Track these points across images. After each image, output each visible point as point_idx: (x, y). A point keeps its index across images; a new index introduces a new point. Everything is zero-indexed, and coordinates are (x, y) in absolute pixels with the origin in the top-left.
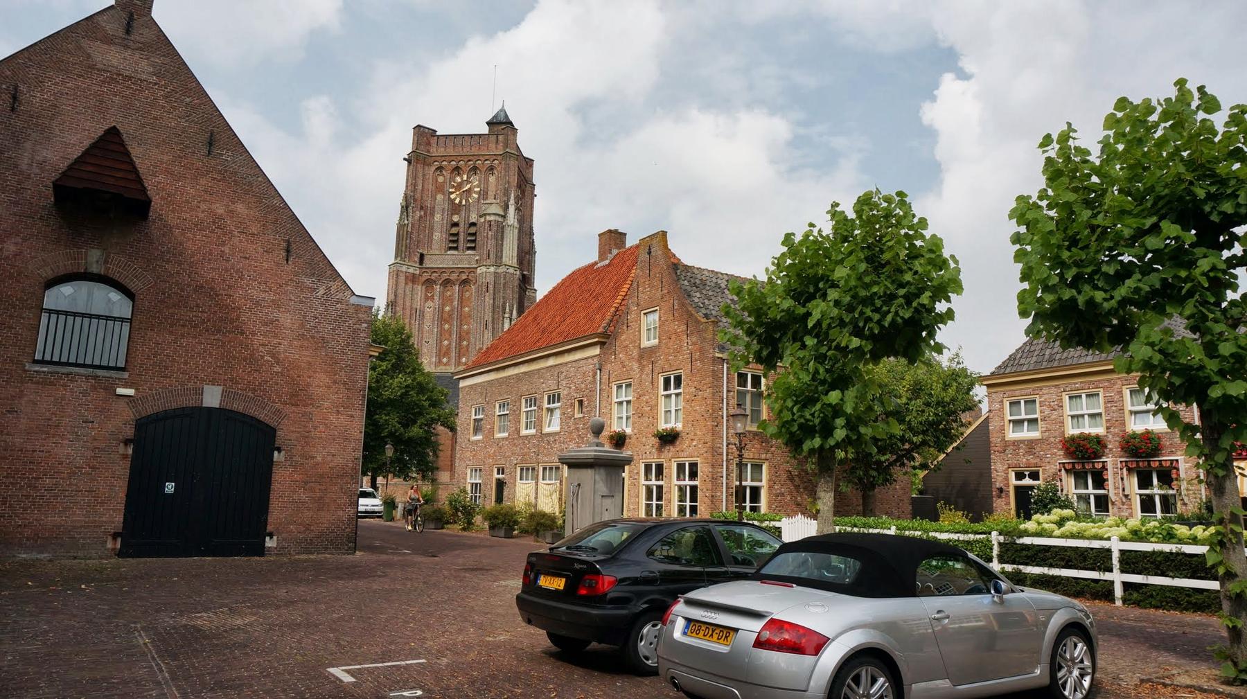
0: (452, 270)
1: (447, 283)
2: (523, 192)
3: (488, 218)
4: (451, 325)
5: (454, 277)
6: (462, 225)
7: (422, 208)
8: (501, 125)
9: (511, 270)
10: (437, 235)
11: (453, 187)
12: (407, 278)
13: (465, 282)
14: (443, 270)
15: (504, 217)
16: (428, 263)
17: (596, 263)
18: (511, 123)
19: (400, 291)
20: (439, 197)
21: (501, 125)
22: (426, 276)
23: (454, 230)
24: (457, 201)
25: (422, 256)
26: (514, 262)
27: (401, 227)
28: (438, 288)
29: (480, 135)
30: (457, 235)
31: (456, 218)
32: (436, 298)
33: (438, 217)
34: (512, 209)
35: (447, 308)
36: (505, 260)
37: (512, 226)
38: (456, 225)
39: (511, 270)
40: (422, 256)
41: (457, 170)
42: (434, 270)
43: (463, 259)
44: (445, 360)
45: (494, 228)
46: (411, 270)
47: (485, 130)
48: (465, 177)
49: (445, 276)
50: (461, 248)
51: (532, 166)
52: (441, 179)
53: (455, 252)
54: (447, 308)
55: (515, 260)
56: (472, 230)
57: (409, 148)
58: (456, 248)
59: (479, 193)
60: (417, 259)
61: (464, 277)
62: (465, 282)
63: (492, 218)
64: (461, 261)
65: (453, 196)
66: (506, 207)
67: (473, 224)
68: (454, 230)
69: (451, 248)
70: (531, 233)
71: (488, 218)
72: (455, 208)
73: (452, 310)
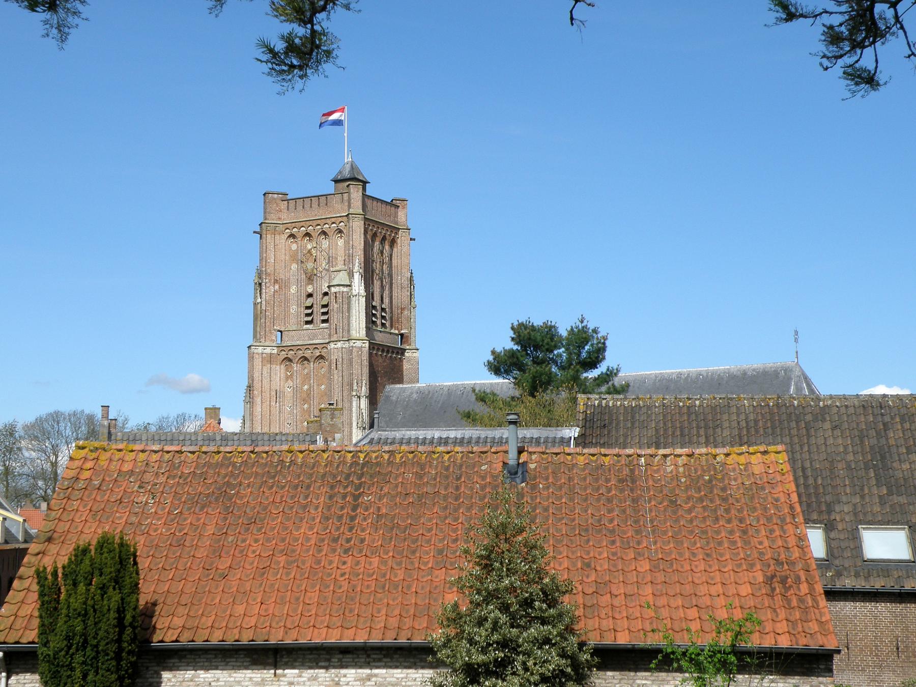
0: (307, 347)
5: (308, 354)
7: (276, 281)
9: (359, 344)
10: (293, 309)
14: (298, 347)
19: (257, 375)
23: (309, 302)
26: (363, 333)
31: (310, 289)
33: (293, 289)
35: (306, 387)
36: (354, 334)
37: (359, 295)
38: (310, 295)
42: (291, 348)
43: (317, 334)
46: (268, 350)
54: (306, 387)
56: (325, 300)
64: (315, 336)
67: (326, 294)
69: (307, 323)
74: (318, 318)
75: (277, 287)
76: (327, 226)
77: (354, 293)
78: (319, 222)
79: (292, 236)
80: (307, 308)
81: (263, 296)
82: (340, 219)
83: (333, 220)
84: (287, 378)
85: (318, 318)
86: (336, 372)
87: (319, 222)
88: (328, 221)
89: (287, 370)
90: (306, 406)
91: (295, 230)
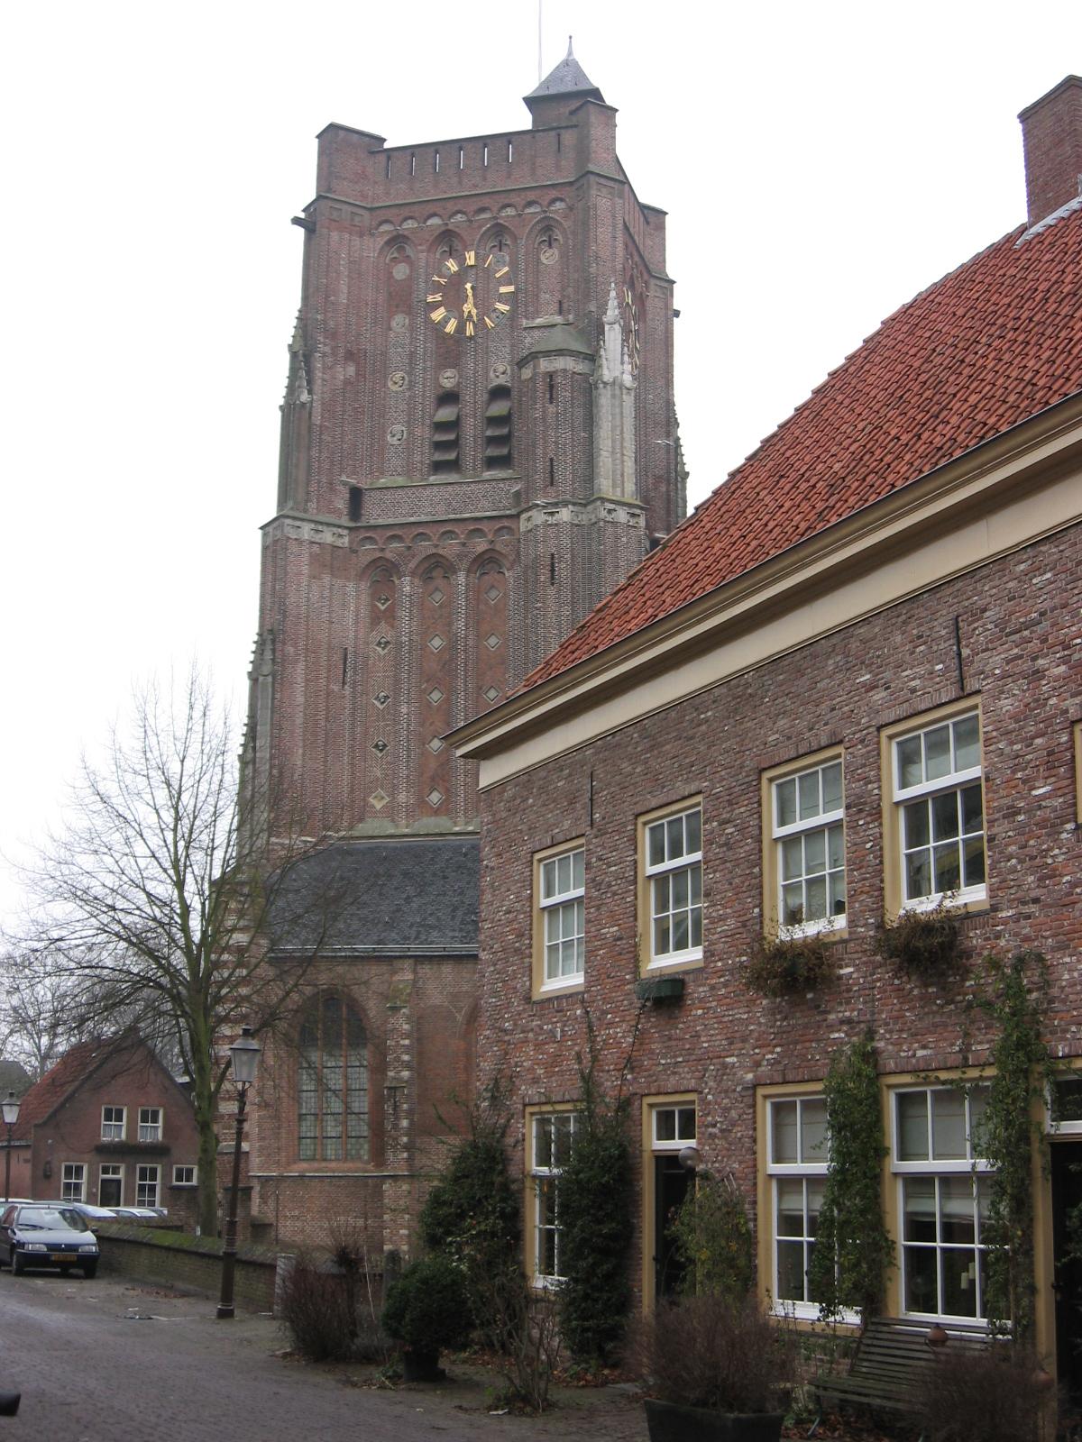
1: (435, 567)
2: (641, 300)
3: (544, 365)
4: (451, 691)
5: (450, 548)
6: (467, 397)
7: (350, 356)
8: (571, 110)
10: (396, 433)
11: (437, 288)
12: (314, 558)
13: (487, 562)
14: (419, 530)
15: (593, 358)
16: (374, 514)
17: (1023, 229)
18: (596, 93)
20: (399, 321)
21: (571, 110)
22: (369, 552)
23: (446, 414)
24: (451, 327)
25: (356, 495)
27: (293, 413)
28: (407, 585)
29: (508, 138)
30: (453, 425)
31: (448, 380)
32: (403, 614)
33: (396, 382)
34: (613, 337)
35: (437, 642)
36: (605, 485)
38: (449, 398)
39: (622, 515)
40: (356, 495)
41: (449, 241)
42: (394, 532)
43: (481, 493)
44: (435, 797)
45: (564, 394)
46: (327, 537)
47: (523, 120)
48: (471, 258)
49: (425, 548)
50: (468, 461)
51: (661, 227)
52: (401, 272)
53: (453, 477)
54: (437, 642)
55: (630, 487)
56: (499, 408)
57: (307, 191)
58: (454, 466)
59: (512, 299)
60: (341, 503)
61: (481, 546)
62: (487, 562)
63: (561, 363)
65: (438, 315)
66: (595, 332)
67: (499, 393)
68: (446, 414)
69: (438, 467)
70: (671, 423)
71: (544, 365)
72: (451, 350)
73: (451, 646)
74: (472, 450)
75: (351, 370)
76: (510, 211)
77: (607, 375)
78: (486, 202)
79: (398, 241)
80: (441, 427)
81: (317, 387)
82: (554, 193)
83: (531, 196)
84: (376, 618)
85: (472, 450)
86: (551, 591)
87: (486, 202)
88: (515, 199)
89: (375, 596)
90: (436, 696)
91: (410, 224)
